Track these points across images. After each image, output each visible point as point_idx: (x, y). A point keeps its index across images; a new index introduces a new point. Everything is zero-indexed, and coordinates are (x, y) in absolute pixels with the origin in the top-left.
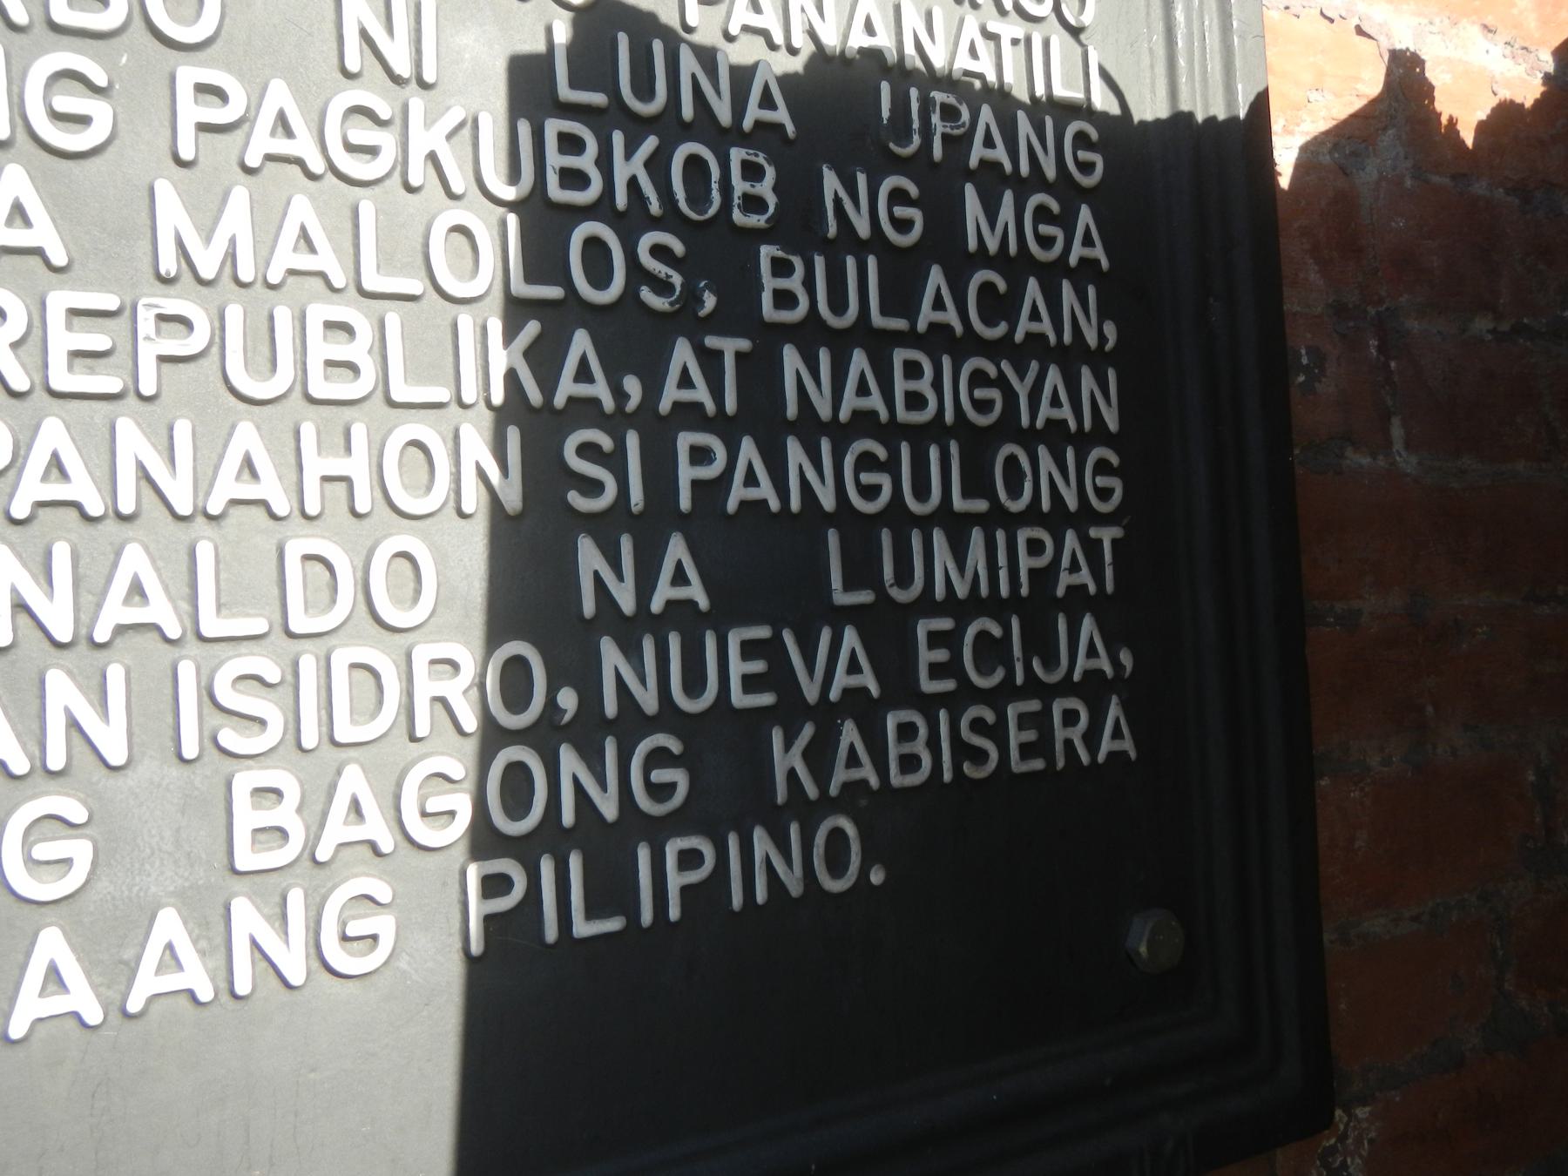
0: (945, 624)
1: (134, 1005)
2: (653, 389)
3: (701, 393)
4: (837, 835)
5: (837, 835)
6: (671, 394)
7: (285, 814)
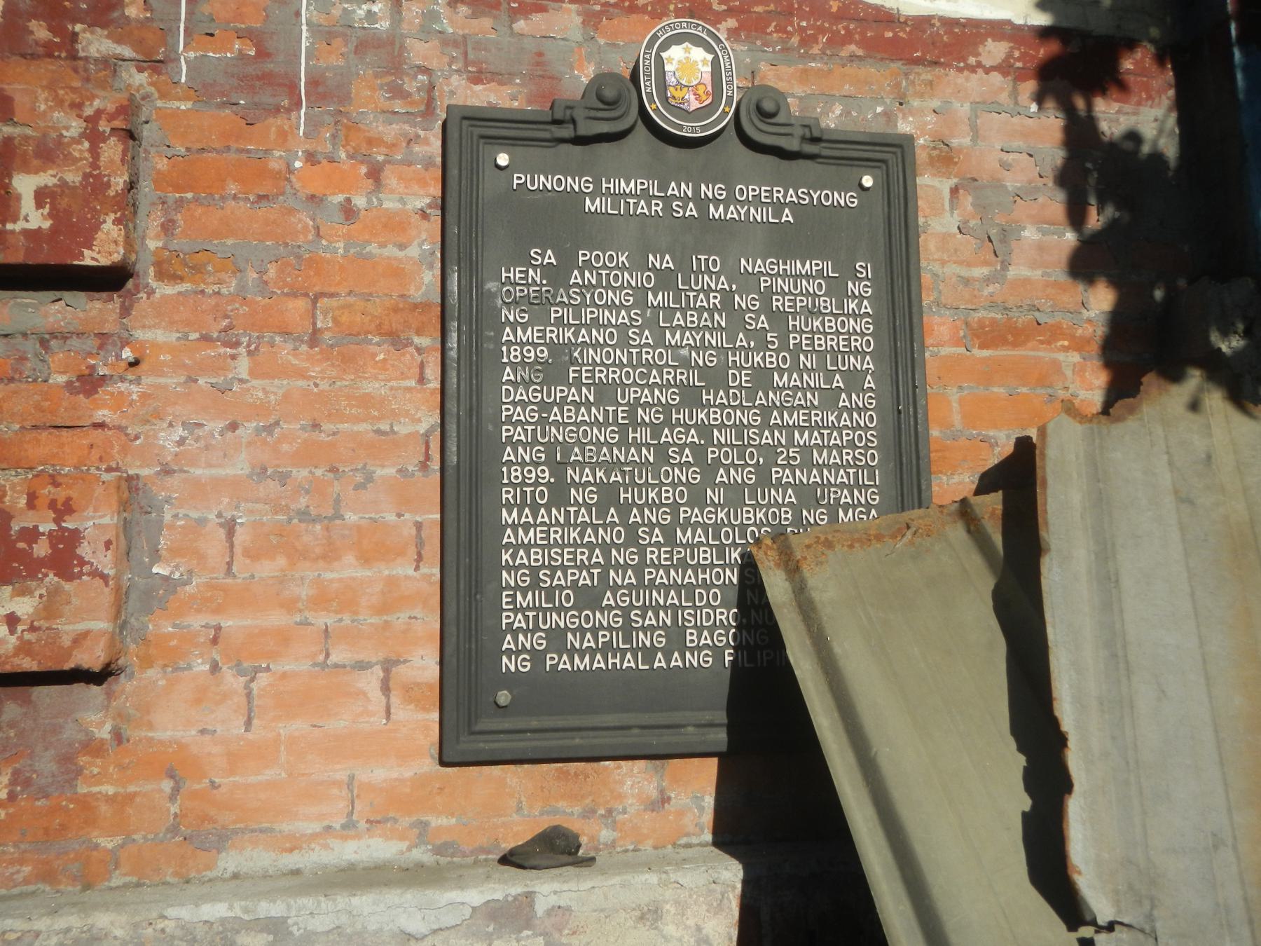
1: (671, 666)
7: (694, 638)
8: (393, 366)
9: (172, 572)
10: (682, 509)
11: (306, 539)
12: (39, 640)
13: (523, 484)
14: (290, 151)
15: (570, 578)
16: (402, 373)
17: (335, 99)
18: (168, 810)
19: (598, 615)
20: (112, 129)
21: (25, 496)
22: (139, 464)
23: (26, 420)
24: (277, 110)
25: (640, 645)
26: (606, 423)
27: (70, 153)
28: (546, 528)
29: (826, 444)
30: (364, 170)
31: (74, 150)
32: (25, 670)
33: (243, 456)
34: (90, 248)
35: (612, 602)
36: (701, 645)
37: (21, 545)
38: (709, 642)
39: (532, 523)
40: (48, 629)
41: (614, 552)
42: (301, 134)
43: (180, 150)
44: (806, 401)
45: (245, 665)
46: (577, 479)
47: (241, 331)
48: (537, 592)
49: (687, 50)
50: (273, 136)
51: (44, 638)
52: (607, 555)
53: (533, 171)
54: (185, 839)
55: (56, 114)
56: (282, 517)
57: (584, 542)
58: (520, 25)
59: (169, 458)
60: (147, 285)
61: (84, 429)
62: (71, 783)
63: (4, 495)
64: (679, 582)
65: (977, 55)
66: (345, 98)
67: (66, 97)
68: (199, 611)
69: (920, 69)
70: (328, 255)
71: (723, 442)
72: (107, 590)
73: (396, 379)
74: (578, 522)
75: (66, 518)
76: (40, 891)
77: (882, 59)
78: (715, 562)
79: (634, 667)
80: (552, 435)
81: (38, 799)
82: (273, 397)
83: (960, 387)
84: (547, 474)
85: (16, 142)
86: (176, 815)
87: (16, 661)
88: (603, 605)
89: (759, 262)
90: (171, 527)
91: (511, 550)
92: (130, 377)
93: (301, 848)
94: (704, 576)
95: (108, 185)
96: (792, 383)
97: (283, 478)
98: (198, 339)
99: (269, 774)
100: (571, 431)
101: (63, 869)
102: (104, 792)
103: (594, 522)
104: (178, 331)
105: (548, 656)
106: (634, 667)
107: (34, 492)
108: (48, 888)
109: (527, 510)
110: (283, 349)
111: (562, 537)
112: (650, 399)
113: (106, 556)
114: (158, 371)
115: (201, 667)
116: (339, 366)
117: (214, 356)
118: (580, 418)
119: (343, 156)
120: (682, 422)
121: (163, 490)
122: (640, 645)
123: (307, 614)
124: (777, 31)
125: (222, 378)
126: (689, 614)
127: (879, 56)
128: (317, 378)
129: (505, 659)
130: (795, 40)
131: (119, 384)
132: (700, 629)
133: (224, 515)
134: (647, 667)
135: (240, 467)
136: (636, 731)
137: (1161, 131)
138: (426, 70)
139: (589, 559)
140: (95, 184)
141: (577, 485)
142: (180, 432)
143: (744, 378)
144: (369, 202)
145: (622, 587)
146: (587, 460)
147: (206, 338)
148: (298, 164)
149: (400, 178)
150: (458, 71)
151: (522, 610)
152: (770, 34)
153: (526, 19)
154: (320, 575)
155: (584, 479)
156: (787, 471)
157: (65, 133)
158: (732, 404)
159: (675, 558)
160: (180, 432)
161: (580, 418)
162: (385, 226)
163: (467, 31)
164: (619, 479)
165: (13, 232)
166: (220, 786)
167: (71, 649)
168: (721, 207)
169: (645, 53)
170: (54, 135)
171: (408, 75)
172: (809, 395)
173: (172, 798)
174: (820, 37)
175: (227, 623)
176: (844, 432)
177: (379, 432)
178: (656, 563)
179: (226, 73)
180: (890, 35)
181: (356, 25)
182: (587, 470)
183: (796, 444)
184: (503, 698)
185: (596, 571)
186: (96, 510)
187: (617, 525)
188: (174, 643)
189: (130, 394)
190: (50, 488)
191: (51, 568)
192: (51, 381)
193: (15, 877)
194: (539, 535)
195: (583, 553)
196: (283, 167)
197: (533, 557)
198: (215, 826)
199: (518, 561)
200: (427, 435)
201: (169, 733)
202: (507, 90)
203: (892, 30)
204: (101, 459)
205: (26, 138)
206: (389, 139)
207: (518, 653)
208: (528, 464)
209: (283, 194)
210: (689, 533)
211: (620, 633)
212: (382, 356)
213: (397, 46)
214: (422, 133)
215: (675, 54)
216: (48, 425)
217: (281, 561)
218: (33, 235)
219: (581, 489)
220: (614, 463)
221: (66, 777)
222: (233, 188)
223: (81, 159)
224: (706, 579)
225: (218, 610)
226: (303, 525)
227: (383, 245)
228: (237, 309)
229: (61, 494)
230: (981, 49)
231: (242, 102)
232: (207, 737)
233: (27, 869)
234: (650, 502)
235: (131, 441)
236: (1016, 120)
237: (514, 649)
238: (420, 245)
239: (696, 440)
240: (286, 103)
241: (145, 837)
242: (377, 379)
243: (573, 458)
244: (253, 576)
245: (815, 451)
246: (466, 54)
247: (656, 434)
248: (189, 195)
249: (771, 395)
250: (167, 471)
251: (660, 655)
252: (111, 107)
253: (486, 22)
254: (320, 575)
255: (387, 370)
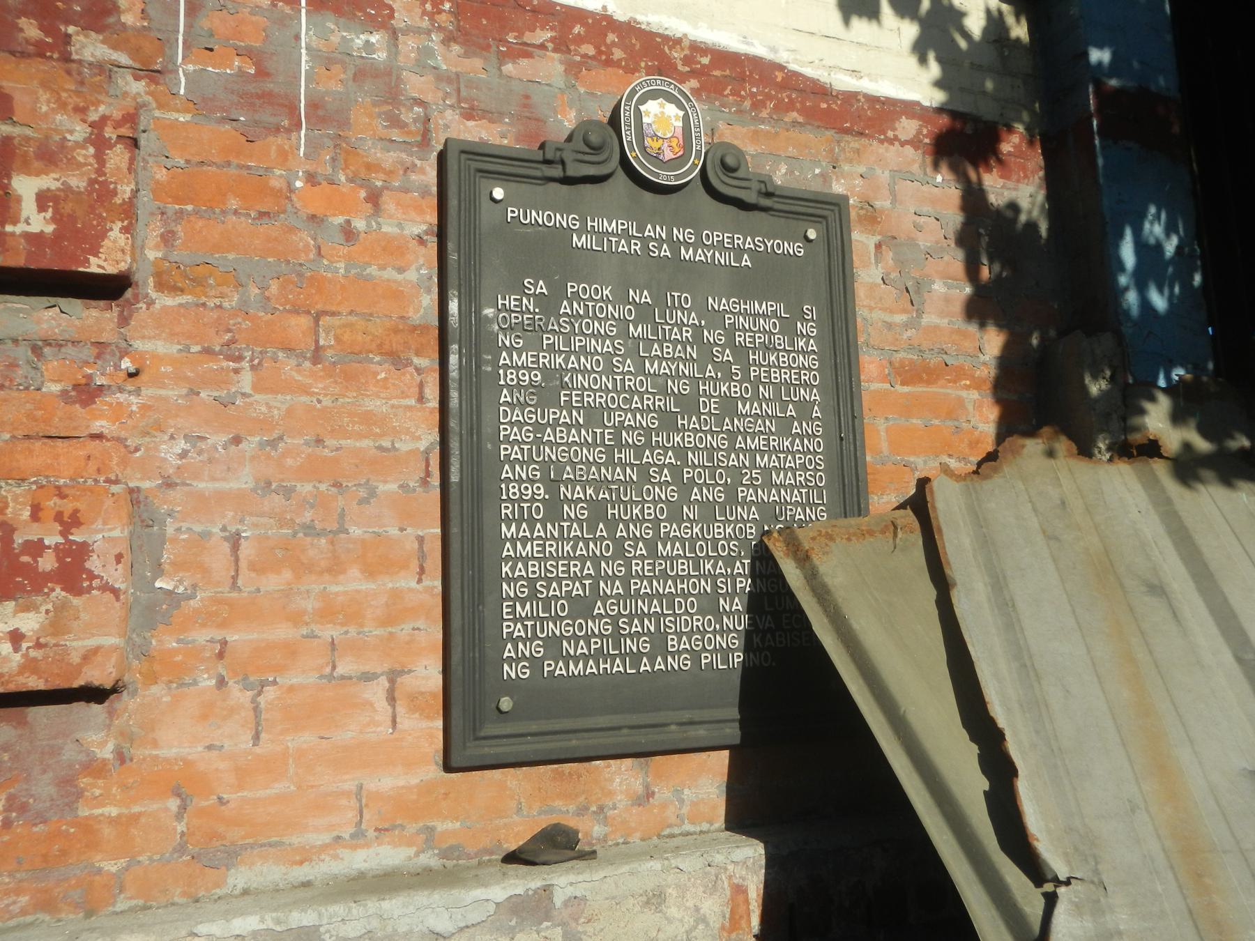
0: (788, 615)
2: (733, 571)
3: (741, 571)
4: (766, 655)
5: (766, 655)
6: (736, 571)
7: (675, 643)
8: (394, 384)
9: (176, 587)
10: (662, 524)
11: (311, 553)
12: (46, 658)
13: (521, 500)
14: (290, 170)
15: (564, 589)
16: (403, 392)
17: (335, 124)
18: (175, 829)
19: (590, 623)
20: (118, 136)
21: (29, 508)
22: (139, 476)
23: (16, 429)
24: (277, 129)
25: (628, 651)
26: (595, 444)
27: (74, 157)
28: (542, 542)
29: (782, 466)
30: (363, 194)
31: (78, 154)
32: (30, 689)
33: (247, 469)
34: (96, 255)
35: (602, 611)
36: (680, 649)
37: (25, 559)
38: (687, 646)
39: (529, 537)
40: (56, 645)
41: (603, 564)
42: (302, 155)
43: (179, 162)
44: (765, 428)
45: (252, 679)
46: (569, 496)
47: (244, 346)
48: (534, 602)
49: (662, 106)
50: (273, 154)
51: (51, 655)
52: (597, 567)
53: (526, 206)
54: (193, 857)
55: (59, 117)
56: (286, 531)
57: (577, 555)
58: (509, 68)
59: (171, 471)
60: (147, 295)
61: (81, 439)
62: (71, 806)
63: (6, 506)
64: (661, 592)
65: (894, 129)
66: (344, 123)
67: (70, 100)
68: (204, 625)
69: (848, 138)
70: (330, 275)
71: (697, 463)
72: (117, 605)
73: (397, 397)
74: (571, 536)
75: (73, 530)
76: (38, 922)
77: (818, 127)
78: (692, 573)
79: (623, 671)
80: (546, 454)
81: (35, 825)
82: (276, 412)
83: (886, 418)
84: (542, 491)
85: (16, 142)
86: (183, 834)
87: (21, 680)
88: (595, 614)
89: (724, 301)
90: (174, 540)
91: (511, 563)
92: (130, 388)
93: (311, 860)
94: (682, 586)
95: (114, 193)
96: (753, 411)
97: (288, 492)
98: (200, 352)
99: (278, 788)
100: (564, 451)
101: (64, 897)
102: (107, 814)
103: (585, 536)
104: (179, 343)
105: (546, 663)
106: (623, 671)
107: (39, 504)
108: (47, 918)
109: (524, 525)
110: (288, 366)
111: (557, 550)
112: (632, 423)
113: (116, 570)
114: (158, 382)
115: (207, 682)
116: (341, 383)
117: (217, 370)
118: (571, 439)
119: (343, 178)
120: (661, 444)
121: (165, 503)
122: (628, 651)
123: (313, 627)
124: (732, 94)
125: (225, 392)
126: (670, 621)
127: (816, 124)
128: (320, 394)
129: (506, 667)
130: (747, 104)
131: (118, 395)
132: (680, 635)
133: (228, 528)
134: (634, 671)
135: (243, 480)
136: (625, 731)
137: (1033, 204)
138: (421, 103)
139: (582, 570)
140: (101, 192)
141: (570, 502)
142: (182, 445)
143: (713, 406)
144: (369, 225)
145: (611, 597)
146: (578, 478)
147: (208, 351)
148: (299, 184)
149: (398, 204)
150: (452, 106)
151: (522, 619)
152: (727, 96)
153: (514, 63)
154: (325, 588)
155: (576, 496)
156: (751, 490)
157: (69, 137)
158: (703, 428)
159: (657, 569)
160: (182, 445)
161: (571, 439)
162: (384, 249)
163: (459, 69)
164: (607, 496)
165: (13, 234)
166: (228, 802)
167: (80, 666)
168: (691, 249)
169: (625, 105)
170: (57, 138)
171: (404, 105)
172: (768, 423)
173: (179, 817)
174: (769, 103)
175: (232, 637)
176: (797, 456)
177: (380, 448)
178: (641, 574)
179: (226, 89)
180: (824, 106)
181: (355, 54)
182: (578, 488)
183: (758, 466)
184: (506, 704)
185: (587, 582)
186: (105, 523)
187: (606, 539)
188: (179, 658)
189: (130, 405)
190: (56, 499)
191: (57, 582)
192: (44, 390)
193: (11, 908)
194: (535, 549)
195: (575, 565)
196: (284, 186)
197: (530, 569)
198: (224, 843)
199: (517, 573)
200: (427, 452)
201: (174, 750)
202: (497, 128)
203: (827, 102)
204: (99, 470)
205: (27, 139)
206: (387, 165)
207: (518, 660)
208: (524, 482)
209: (284, 212)
210: (669, 547)
211: (610, 640)
212: (383, 375)
213: (394, 79)
214: (418, 163)
215: (652, 109)
216: (41, 434)
217: (287, 575)
218: (35, 239)
219: (573, 505)
220: (602, 482)
221: (66, 800)
222: (233, 203)
223: (86, 164)
224: (684, 589)
225: (223, 625)
226: (309, 539)
227: (382, 268)
228: (239, 323)
229: (68, 506)
230: (897, 125)
231: (242, 119)
232: (215, 753)
233: (24, 900)
234: (634, 518)
235: (131, 453)
236: (925, 188)
237: (514, 657)
238: (418, 270)
239: (673, 461)
240: (286, 123)
241: (150, 859)
242: (379, 397)
243: (565, 476)
244: (258, 590)
245: (773, 472)
246: (458, 91)
247: (639, 456)
248: (189, 208)
249: (736, 421)
250: (169, 484)
251: (645, 660)
252: (117, 115)
253: (477, 63)
254: (325, 588)
255: (387, 388)
